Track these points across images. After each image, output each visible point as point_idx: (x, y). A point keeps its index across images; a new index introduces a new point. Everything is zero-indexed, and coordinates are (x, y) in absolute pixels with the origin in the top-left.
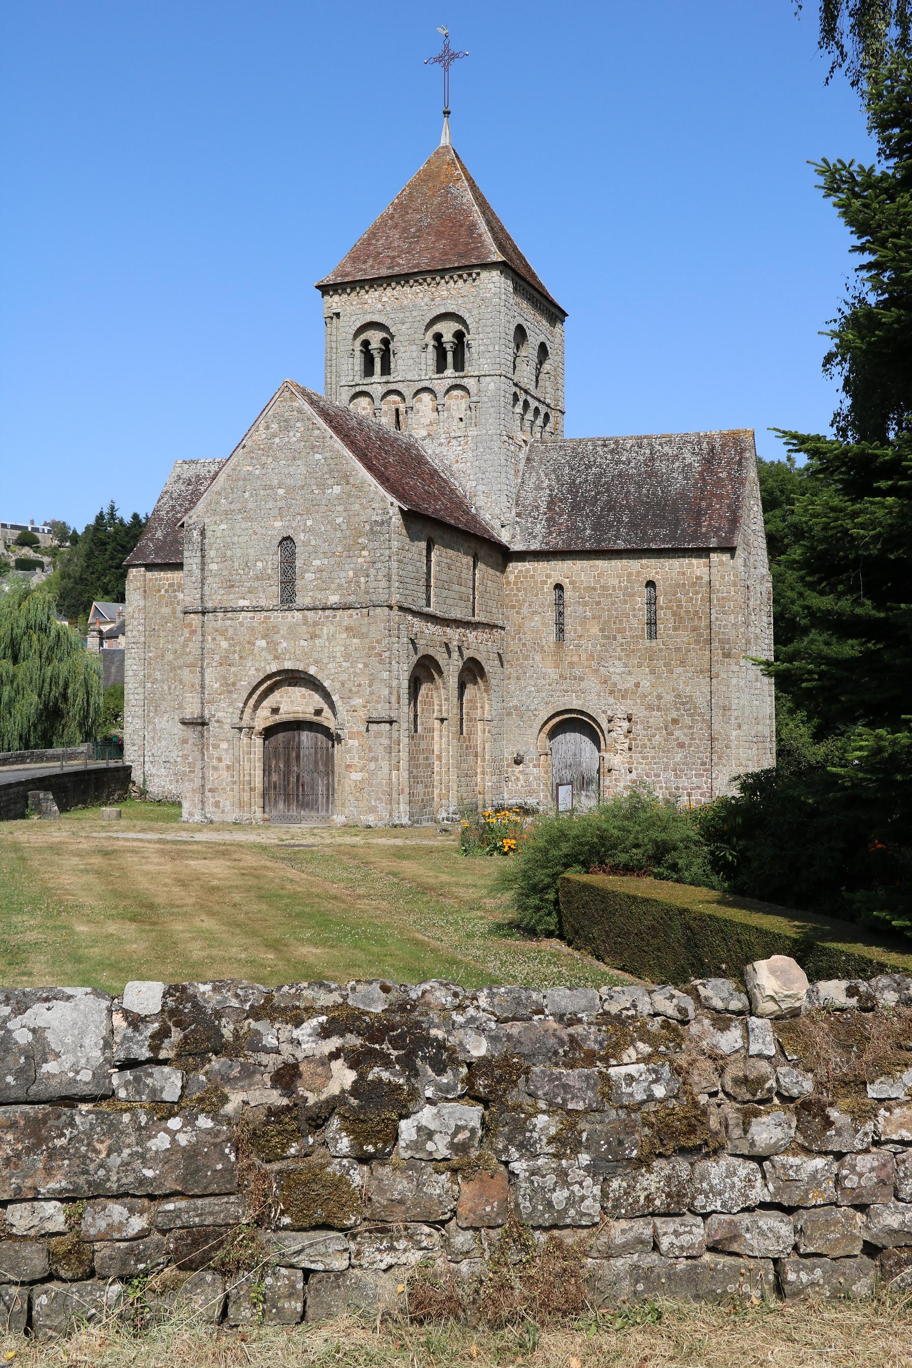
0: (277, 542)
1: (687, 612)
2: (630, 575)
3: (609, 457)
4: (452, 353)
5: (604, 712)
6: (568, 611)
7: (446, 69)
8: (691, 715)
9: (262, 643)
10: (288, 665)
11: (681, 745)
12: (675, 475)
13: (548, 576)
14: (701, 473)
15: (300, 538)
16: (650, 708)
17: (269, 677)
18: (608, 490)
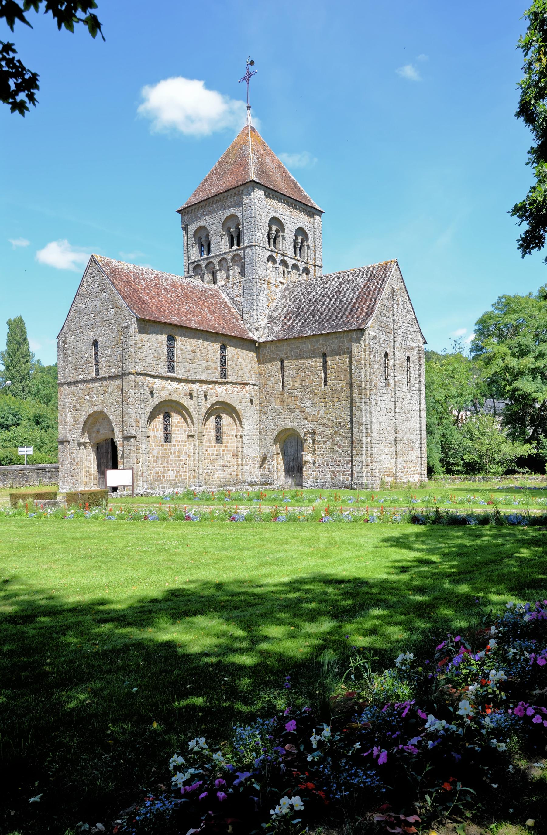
0: (91, 343)
1: (342, 369)
2: (314, 350)
3: (321, 286)
4: (236, 238)
5: (303, 429)
6: (286, 374)
7: (248, 82)
8: (343, 429)
9: (87, 397)
10: (96, 408)
11: (339, 447)
12: (349, 291)
13: (277, 355)
14: (362, 289)
15: (100, 339)
16: (325, 425)
17: (90, 415)
18: (315, 304)
